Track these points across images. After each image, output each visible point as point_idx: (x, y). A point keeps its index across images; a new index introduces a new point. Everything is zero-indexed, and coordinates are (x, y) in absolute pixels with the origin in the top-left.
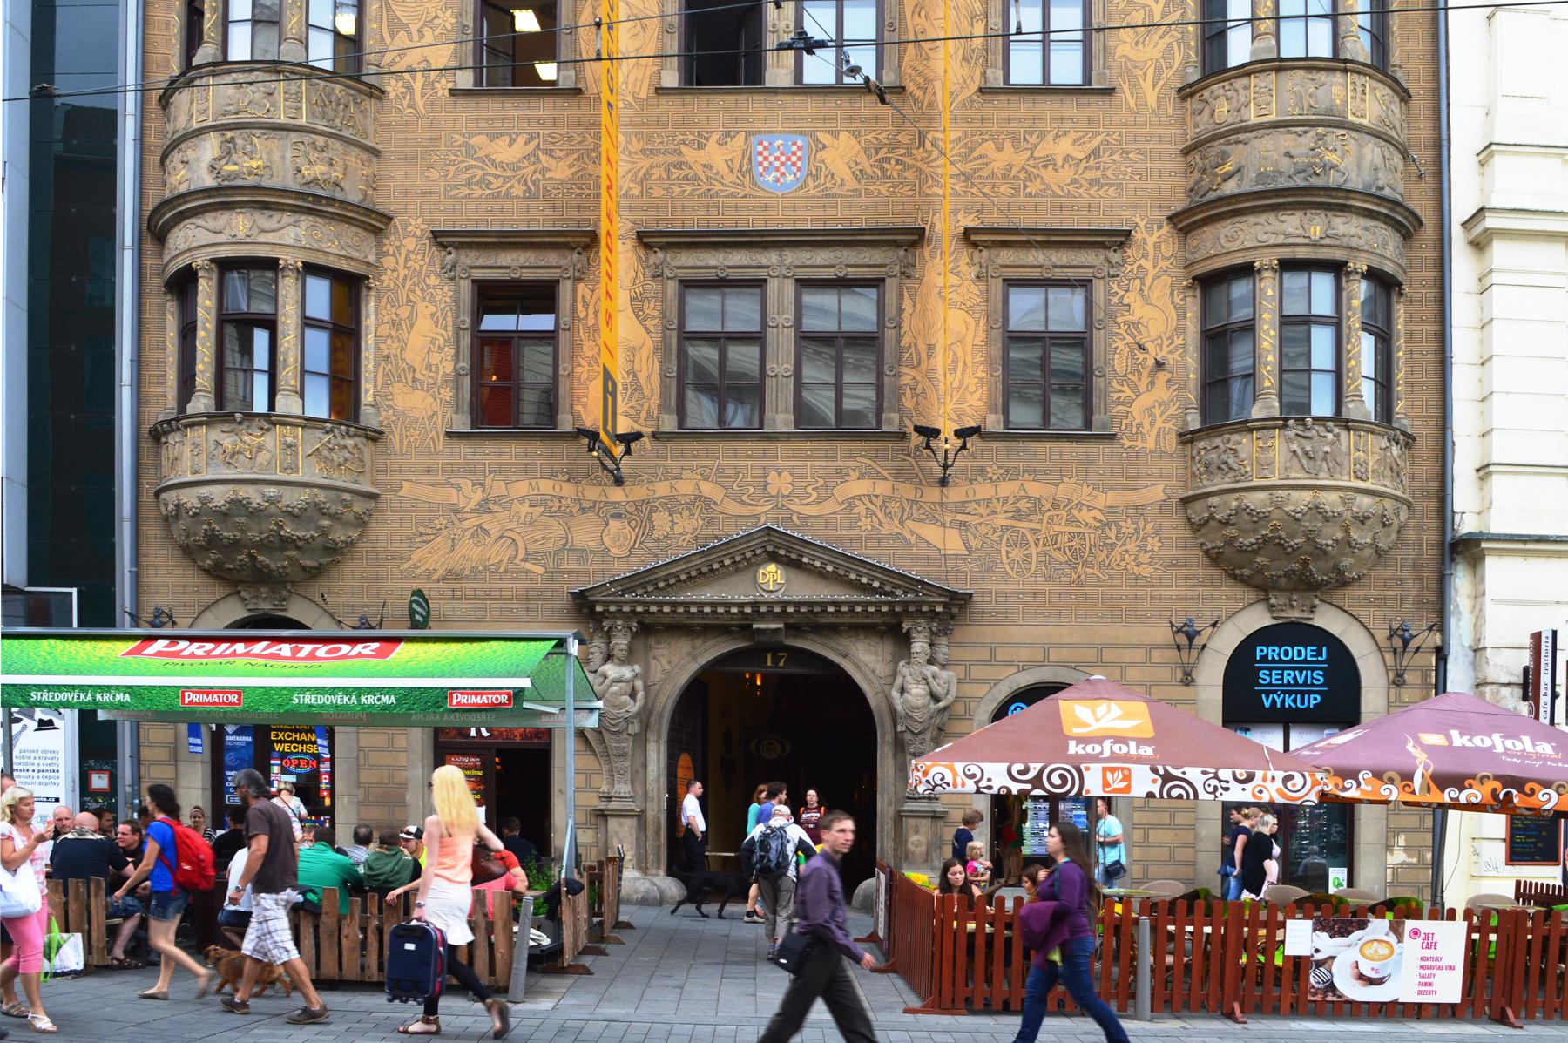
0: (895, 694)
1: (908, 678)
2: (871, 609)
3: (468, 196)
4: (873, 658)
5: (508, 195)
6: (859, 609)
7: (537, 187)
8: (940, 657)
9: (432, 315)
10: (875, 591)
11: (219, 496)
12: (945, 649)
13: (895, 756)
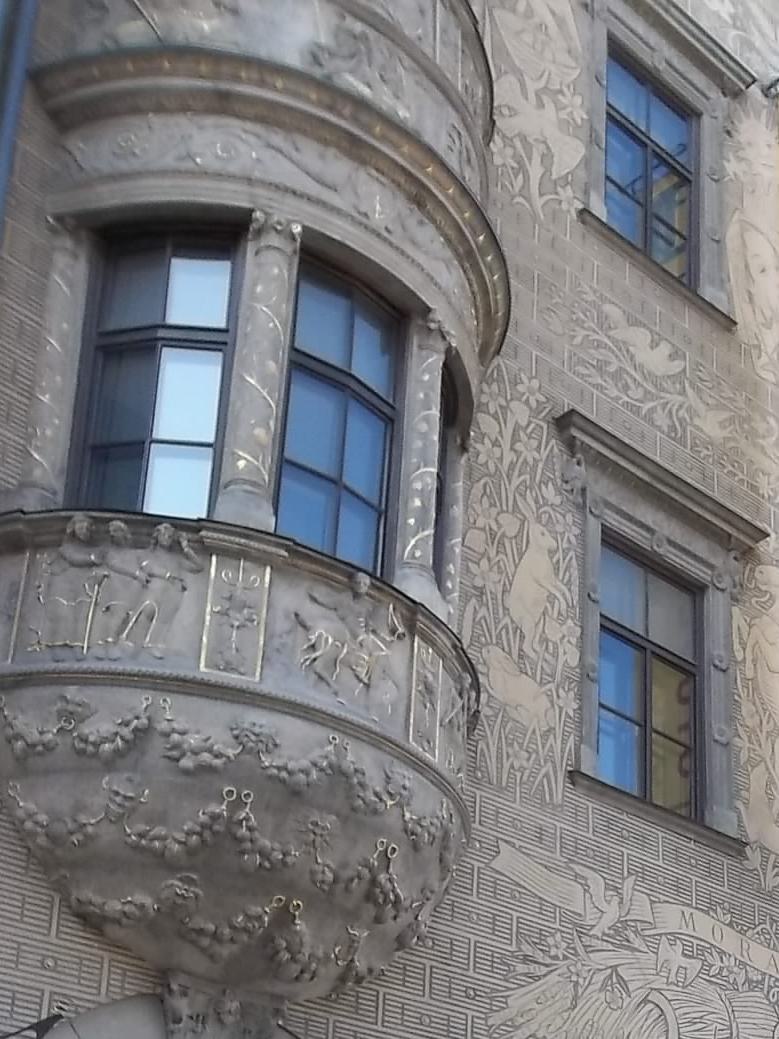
3: (597, 386)
5: (649, 418)
7: (684, 431)
9: (552, 553)
11: (298, 747)
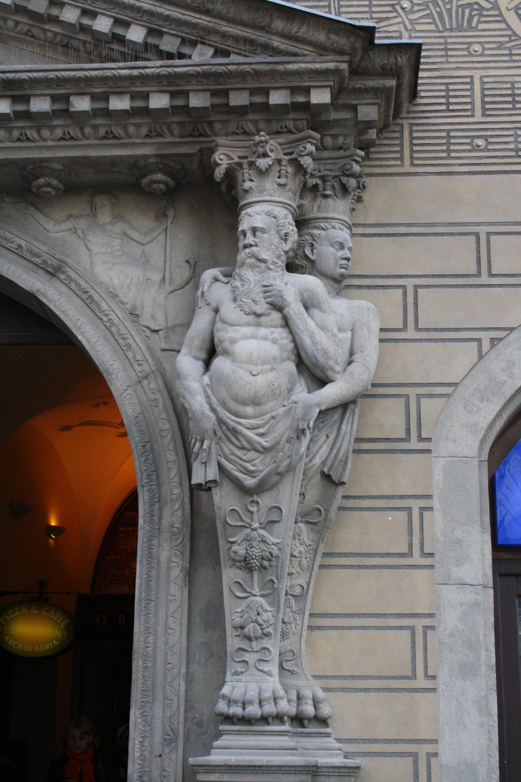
0: (188, 364)
1: (229, 310)
2: (120, 103)
4: (136, 274)
6: (82, 104)
8: (328, 255)
10: (138, 52)
12: (343, 234)
13: (190, 575)
